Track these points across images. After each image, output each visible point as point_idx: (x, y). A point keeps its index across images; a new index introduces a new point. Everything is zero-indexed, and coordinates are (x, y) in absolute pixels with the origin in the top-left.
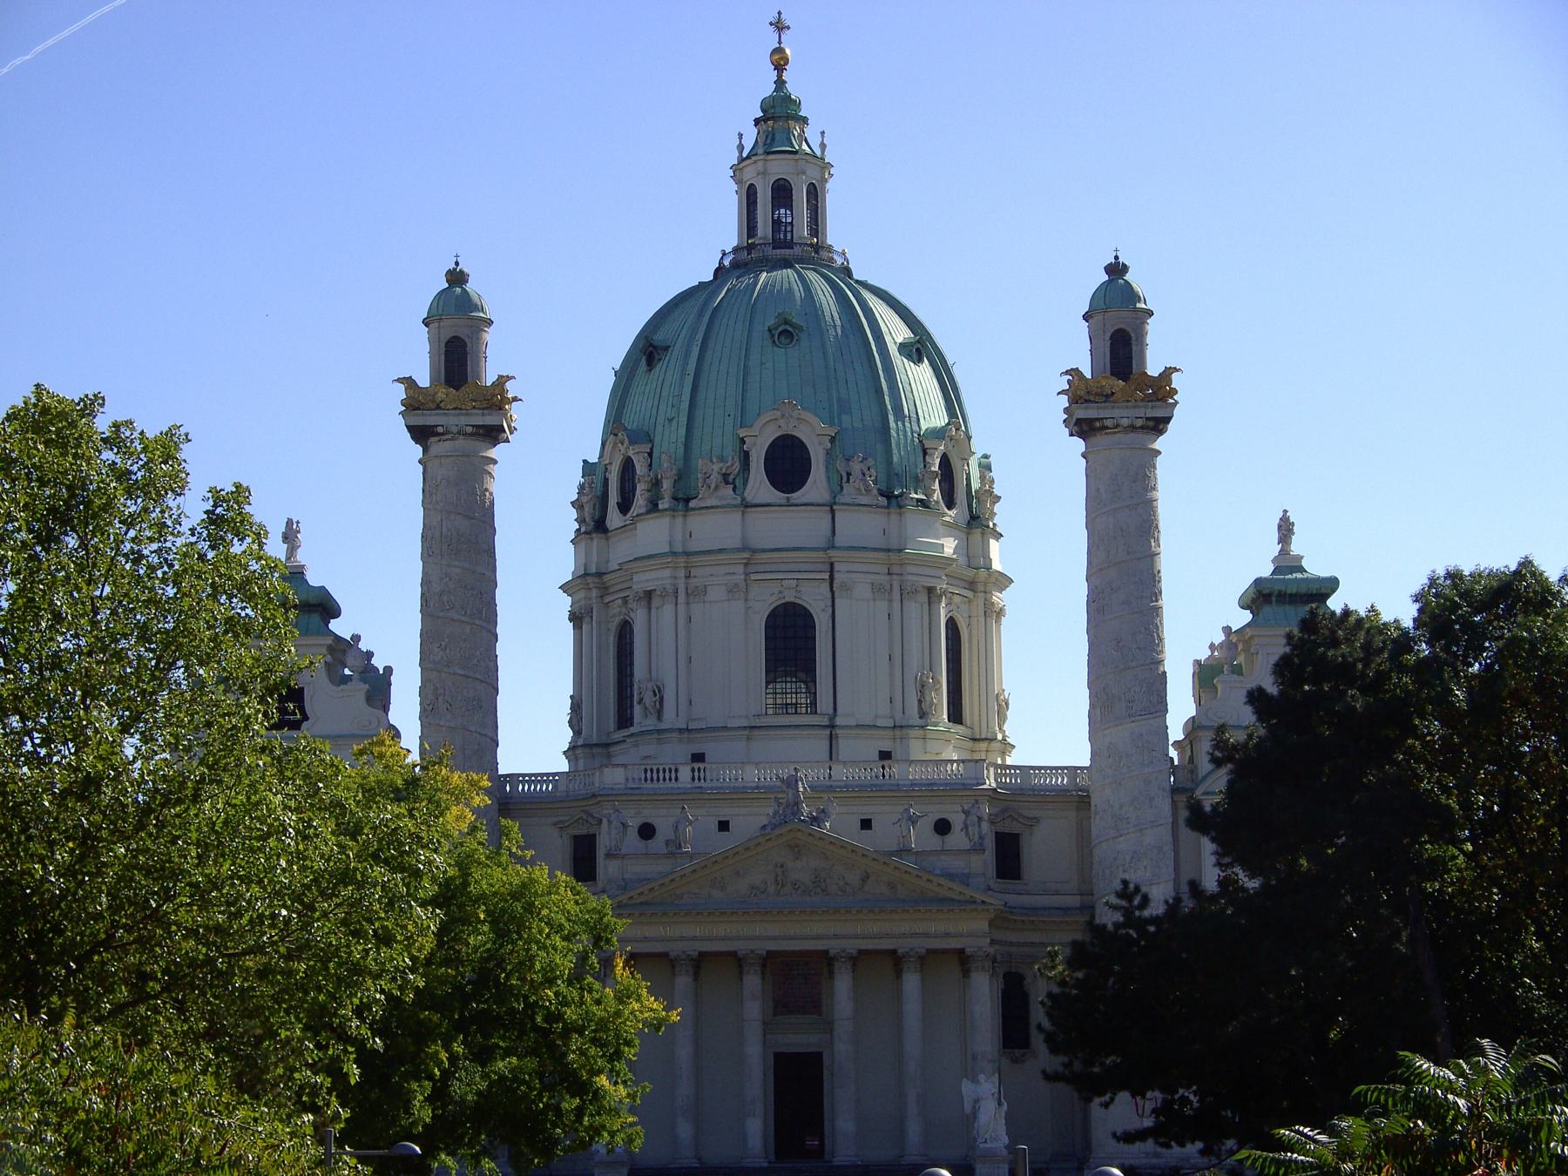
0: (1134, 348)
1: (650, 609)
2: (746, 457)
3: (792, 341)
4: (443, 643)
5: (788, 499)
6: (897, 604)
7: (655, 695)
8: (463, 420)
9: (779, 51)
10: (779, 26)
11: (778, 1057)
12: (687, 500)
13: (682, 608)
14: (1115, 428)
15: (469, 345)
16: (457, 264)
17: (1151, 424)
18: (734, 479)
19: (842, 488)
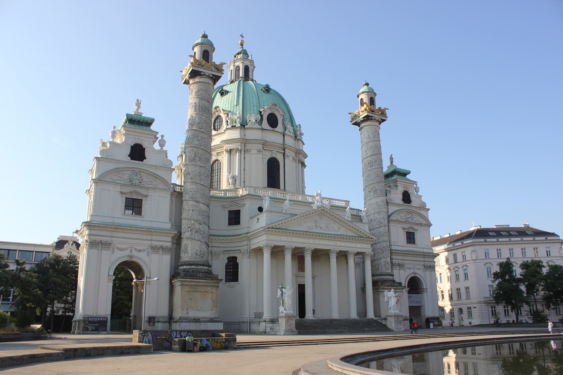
0: (375, 103)
1: (230, 155)
2: (262, 116)
3: (268, 92)
4: (199, 139)
5: (273, 130)
6: (297, 164)
7: (233, 177)
8: (210, 72)
9: (242, 41)
10: (243, 37)
11: (298, 284)
12: (244, 126)
13: (243, 154)
14: (374, 120)
15: (210, 54)
16: (204, 33)
17: (381, 121)
18: (258, 122)
19: (285, 130)
